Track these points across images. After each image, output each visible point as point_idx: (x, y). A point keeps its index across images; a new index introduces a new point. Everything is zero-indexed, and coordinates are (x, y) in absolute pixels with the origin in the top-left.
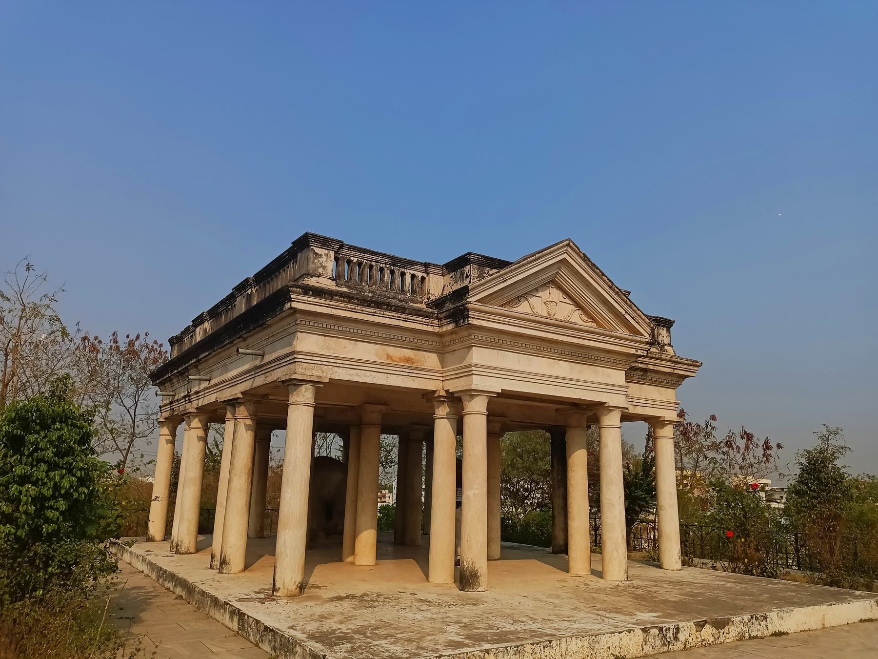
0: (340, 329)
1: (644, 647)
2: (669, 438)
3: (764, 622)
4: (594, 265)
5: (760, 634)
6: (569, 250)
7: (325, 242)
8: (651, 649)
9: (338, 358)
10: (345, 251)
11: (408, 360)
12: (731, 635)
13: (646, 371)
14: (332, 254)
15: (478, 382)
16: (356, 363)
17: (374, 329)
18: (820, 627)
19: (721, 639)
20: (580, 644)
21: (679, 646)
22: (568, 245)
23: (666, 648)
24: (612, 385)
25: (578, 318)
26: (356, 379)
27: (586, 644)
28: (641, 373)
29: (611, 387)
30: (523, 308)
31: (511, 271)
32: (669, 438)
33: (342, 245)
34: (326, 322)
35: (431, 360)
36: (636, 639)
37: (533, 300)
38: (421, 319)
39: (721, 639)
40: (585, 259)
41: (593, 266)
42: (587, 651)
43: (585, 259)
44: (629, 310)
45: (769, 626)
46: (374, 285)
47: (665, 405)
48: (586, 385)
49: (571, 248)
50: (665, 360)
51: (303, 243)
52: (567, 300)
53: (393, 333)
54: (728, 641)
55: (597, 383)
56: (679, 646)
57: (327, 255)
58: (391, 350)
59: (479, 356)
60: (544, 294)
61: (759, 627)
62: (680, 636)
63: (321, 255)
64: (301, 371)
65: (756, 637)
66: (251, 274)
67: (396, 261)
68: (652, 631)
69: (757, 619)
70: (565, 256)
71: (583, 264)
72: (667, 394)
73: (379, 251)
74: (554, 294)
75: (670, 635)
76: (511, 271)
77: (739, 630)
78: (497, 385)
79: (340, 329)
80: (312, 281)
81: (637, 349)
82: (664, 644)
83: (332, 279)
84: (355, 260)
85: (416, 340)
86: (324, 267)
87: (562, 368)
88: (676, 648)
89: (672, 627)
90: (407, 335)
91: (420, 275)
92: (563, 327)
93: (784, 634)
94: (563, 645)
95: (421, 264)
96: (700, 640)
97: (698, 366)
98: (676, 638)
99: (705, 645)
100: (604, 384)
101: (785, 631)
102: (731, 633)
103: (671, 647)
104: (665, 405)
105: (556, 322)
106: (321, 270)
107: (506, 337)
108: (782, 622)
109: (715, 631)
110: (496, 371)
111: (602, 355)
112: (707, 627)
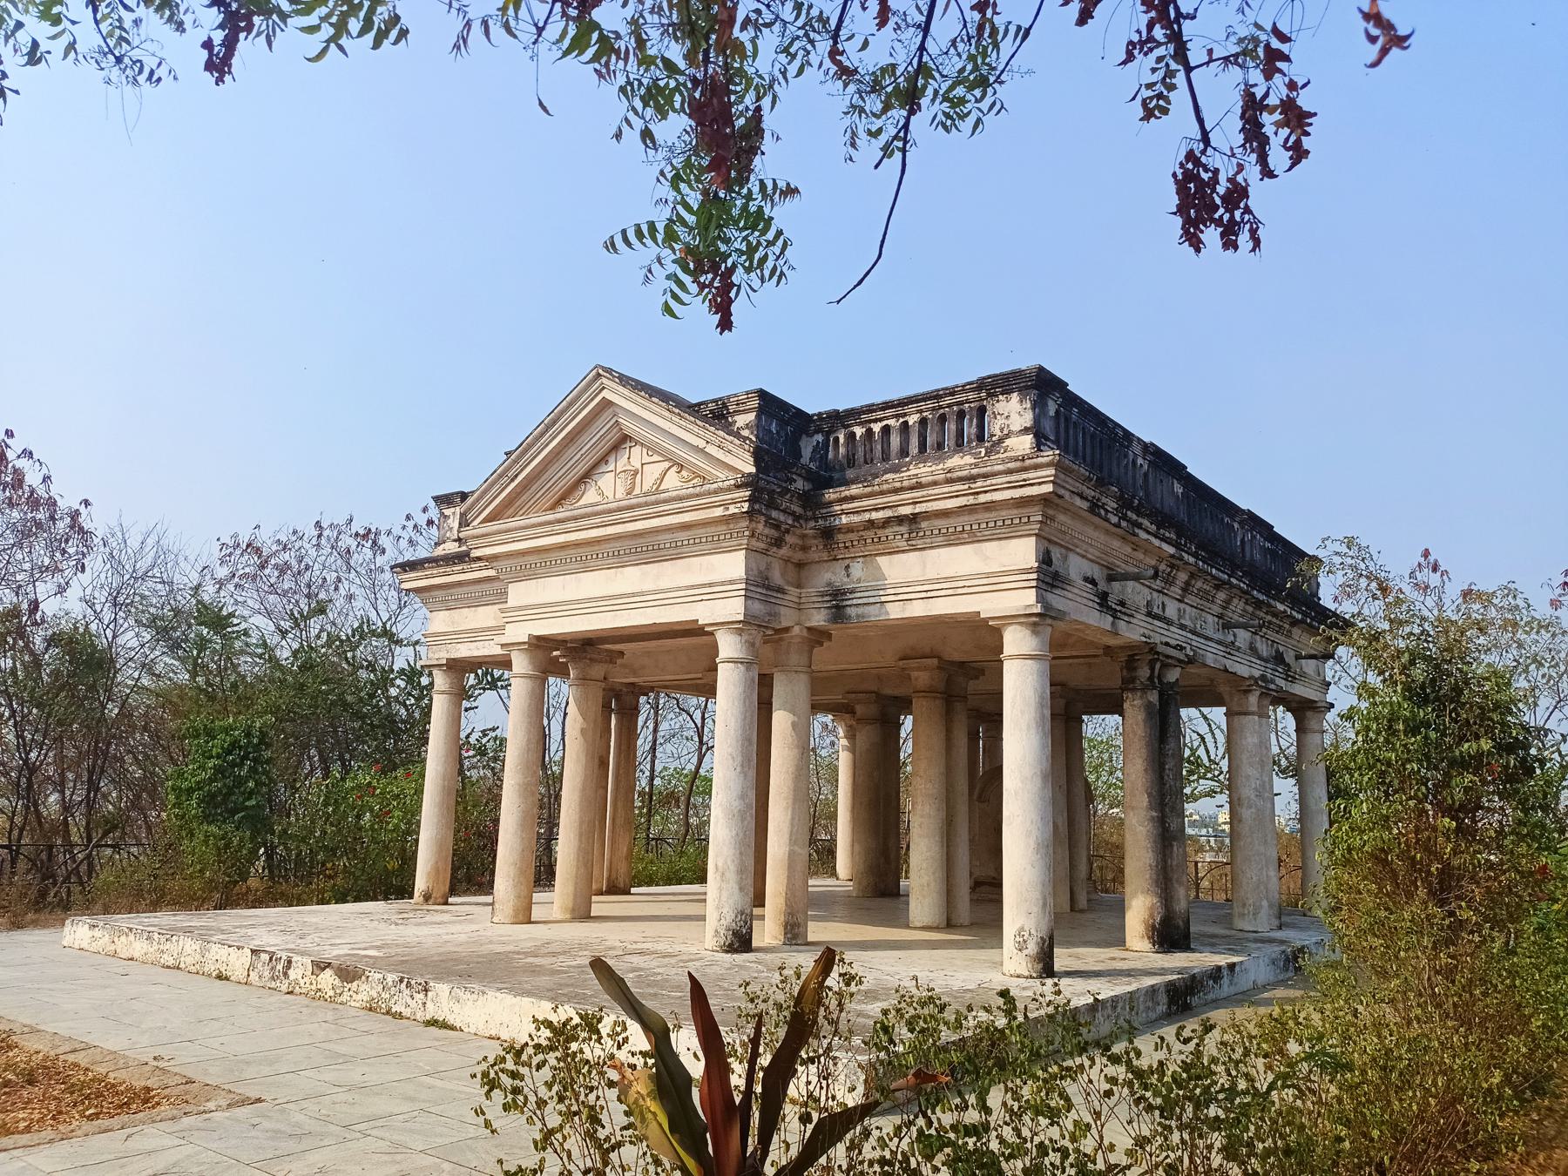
3: (422, 996)
5: (406, 1012)
6: (604, 380)
12: (359, 997)
13: (913, 519)
19: (344, 998)
24: (711, 585)
28: (904, 529)
29: (710, 590)
30: (590, 496)
32: (1011, 657)
39: (344, 998)
45: (429, 1005)
48: (661, 597)
50: (935, 483)
55: (679, 589)
60: (621, 462)
61: (409, 1000)
62: (291, 972)
65: (400, 1016)
69: (409, 985)
75: (280, 967)
81: (725, 506)
87: (631, 578)
93: (453, 1028)
99: (318, 996)
100: (693, 587)
102: (364, 991)
108: (456, 1007)
109: (337, 982)
112: (328, 972)
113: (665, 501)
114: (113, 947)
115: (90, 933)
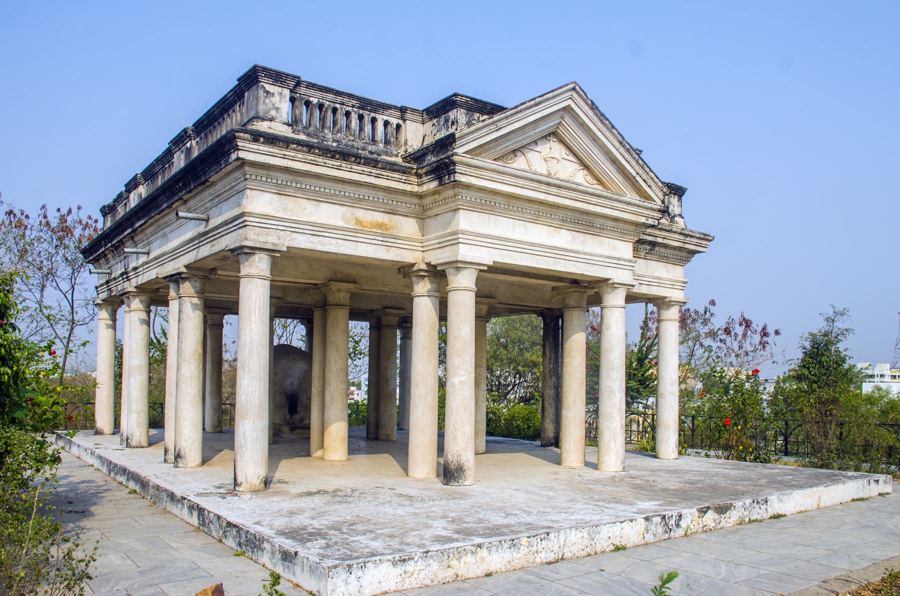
0: (299, 186)
1: (646, 535)
2: (675, 320)
4: (603, 115)
5: (759, 517)
7: (278, 77)
8: (652, 537)
9: (296, 222)
10: (302, 90)
11: (381, 225)
12: (731, 520)
13: (653, 244)
14: (287, 92)
15: (465, 252)
16: (319, 229)
17: (340, 187)
18: (815, 507)
19: (722, 524)
20: (579, 535)
21: (680, 532)
22: (574, 89)
23: (667, 536)
24: (619, 259)
25: (581, 177)
26: (319, 248)
27: (586, 535)
28: (648, 247)
29: (617, 262)
30: (519, 163)
31: (507, 118)
32: (675, 320)
33: (299, 83)
34: (281, 177)
35: (408, 226)
36: (639, 526)
37: (531, 155)
38: (396, 175)
39: (722, 524)
40: (593, 107)
41: (602, 117)
42: (586, 542)
43: (593, 107)
44: (640, 171)
45: (769, 509)
46: (339, 131)
47: (672, 284)
48: (589, 258)
49: (577, 93)
50: (675, 232)
51: (250, 80)
52: (571, 157)
53: (363, 191)
54: (728, 525)
55: (601, 256)
56: (680, 532)
57: (281, 94)
58: (362, 214)
59: (468, 221)
62: (683, 523)
63: (273, 94)
64: (252, 237)
65: (756, 521)
66: (189, 123)
67: (366, 104)
68: (654, 519)
69: (758, 503)
70: (570, 102)
71: (591, 113)
72: (675, 272)
73: (345, 91)
74: (554, 148)
75: (673, 522)
76: (507, 118)
77: (740, 514)
78: (487, 256)
79: (299, 186)
80: (262, 126)
81: (647, 217)
82: (666, 532)
83: (288, 124)
84: (315, 101)
85: (391, 203)
86: (277, 109)
87: (563, 238)
88: (677, 535)
89: (675, 514)
90: (381, 195)
91: (394, 121)
92: (566, 188)
94: (562, 537)
95: (396, 108)
96: (701, 526)
97: (710, 241)
98: (678, 525)
99: (706, 530)
100: (609, 257)
101: (783, 513)
102: (733, 517)
103: (672, 534)
104: (672, 284)
105: (559, 182)
106: (273, 113)
107: (499, 199)
108: (781, 505)
109: (716, 516)
110: (487, 238)
111: (610, 223)
112: (710, 512)
113: (620, 202)
114: (450, 573)
115: (399, 570)
